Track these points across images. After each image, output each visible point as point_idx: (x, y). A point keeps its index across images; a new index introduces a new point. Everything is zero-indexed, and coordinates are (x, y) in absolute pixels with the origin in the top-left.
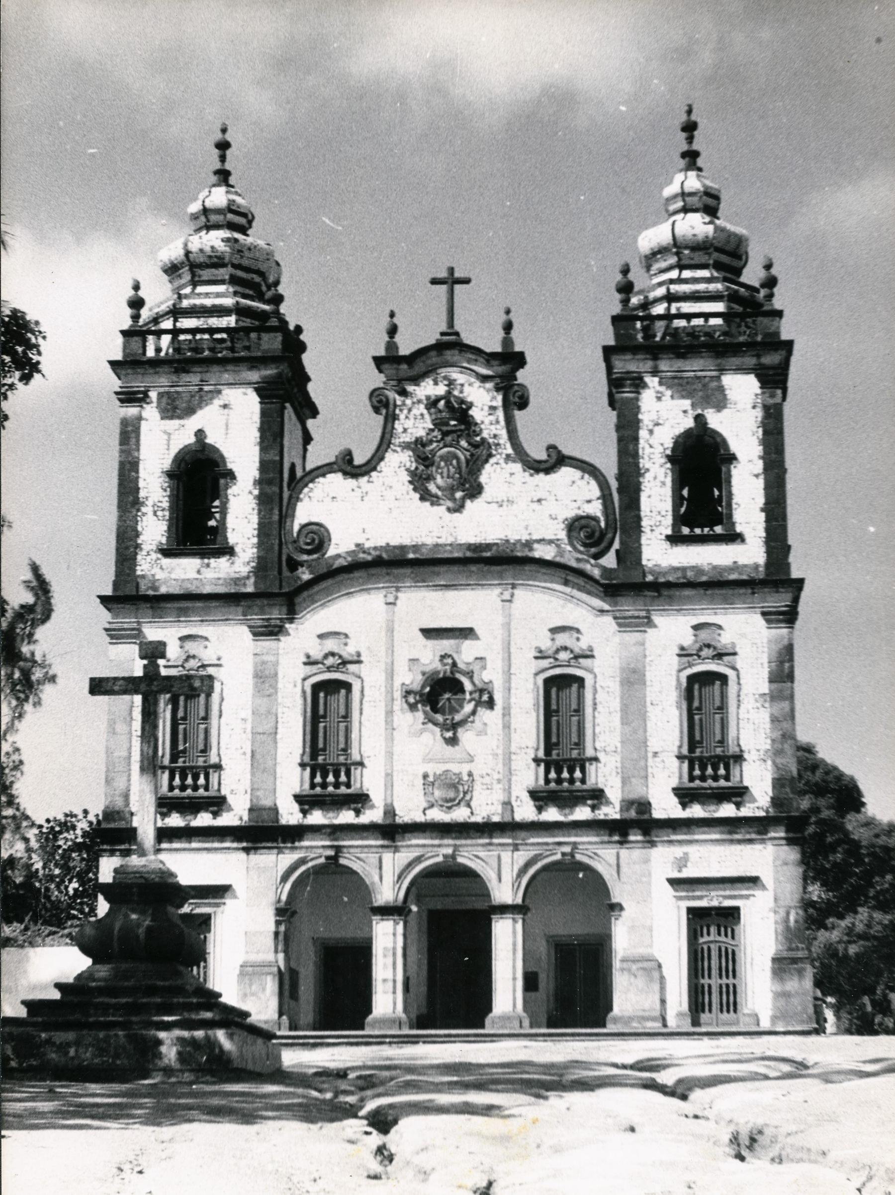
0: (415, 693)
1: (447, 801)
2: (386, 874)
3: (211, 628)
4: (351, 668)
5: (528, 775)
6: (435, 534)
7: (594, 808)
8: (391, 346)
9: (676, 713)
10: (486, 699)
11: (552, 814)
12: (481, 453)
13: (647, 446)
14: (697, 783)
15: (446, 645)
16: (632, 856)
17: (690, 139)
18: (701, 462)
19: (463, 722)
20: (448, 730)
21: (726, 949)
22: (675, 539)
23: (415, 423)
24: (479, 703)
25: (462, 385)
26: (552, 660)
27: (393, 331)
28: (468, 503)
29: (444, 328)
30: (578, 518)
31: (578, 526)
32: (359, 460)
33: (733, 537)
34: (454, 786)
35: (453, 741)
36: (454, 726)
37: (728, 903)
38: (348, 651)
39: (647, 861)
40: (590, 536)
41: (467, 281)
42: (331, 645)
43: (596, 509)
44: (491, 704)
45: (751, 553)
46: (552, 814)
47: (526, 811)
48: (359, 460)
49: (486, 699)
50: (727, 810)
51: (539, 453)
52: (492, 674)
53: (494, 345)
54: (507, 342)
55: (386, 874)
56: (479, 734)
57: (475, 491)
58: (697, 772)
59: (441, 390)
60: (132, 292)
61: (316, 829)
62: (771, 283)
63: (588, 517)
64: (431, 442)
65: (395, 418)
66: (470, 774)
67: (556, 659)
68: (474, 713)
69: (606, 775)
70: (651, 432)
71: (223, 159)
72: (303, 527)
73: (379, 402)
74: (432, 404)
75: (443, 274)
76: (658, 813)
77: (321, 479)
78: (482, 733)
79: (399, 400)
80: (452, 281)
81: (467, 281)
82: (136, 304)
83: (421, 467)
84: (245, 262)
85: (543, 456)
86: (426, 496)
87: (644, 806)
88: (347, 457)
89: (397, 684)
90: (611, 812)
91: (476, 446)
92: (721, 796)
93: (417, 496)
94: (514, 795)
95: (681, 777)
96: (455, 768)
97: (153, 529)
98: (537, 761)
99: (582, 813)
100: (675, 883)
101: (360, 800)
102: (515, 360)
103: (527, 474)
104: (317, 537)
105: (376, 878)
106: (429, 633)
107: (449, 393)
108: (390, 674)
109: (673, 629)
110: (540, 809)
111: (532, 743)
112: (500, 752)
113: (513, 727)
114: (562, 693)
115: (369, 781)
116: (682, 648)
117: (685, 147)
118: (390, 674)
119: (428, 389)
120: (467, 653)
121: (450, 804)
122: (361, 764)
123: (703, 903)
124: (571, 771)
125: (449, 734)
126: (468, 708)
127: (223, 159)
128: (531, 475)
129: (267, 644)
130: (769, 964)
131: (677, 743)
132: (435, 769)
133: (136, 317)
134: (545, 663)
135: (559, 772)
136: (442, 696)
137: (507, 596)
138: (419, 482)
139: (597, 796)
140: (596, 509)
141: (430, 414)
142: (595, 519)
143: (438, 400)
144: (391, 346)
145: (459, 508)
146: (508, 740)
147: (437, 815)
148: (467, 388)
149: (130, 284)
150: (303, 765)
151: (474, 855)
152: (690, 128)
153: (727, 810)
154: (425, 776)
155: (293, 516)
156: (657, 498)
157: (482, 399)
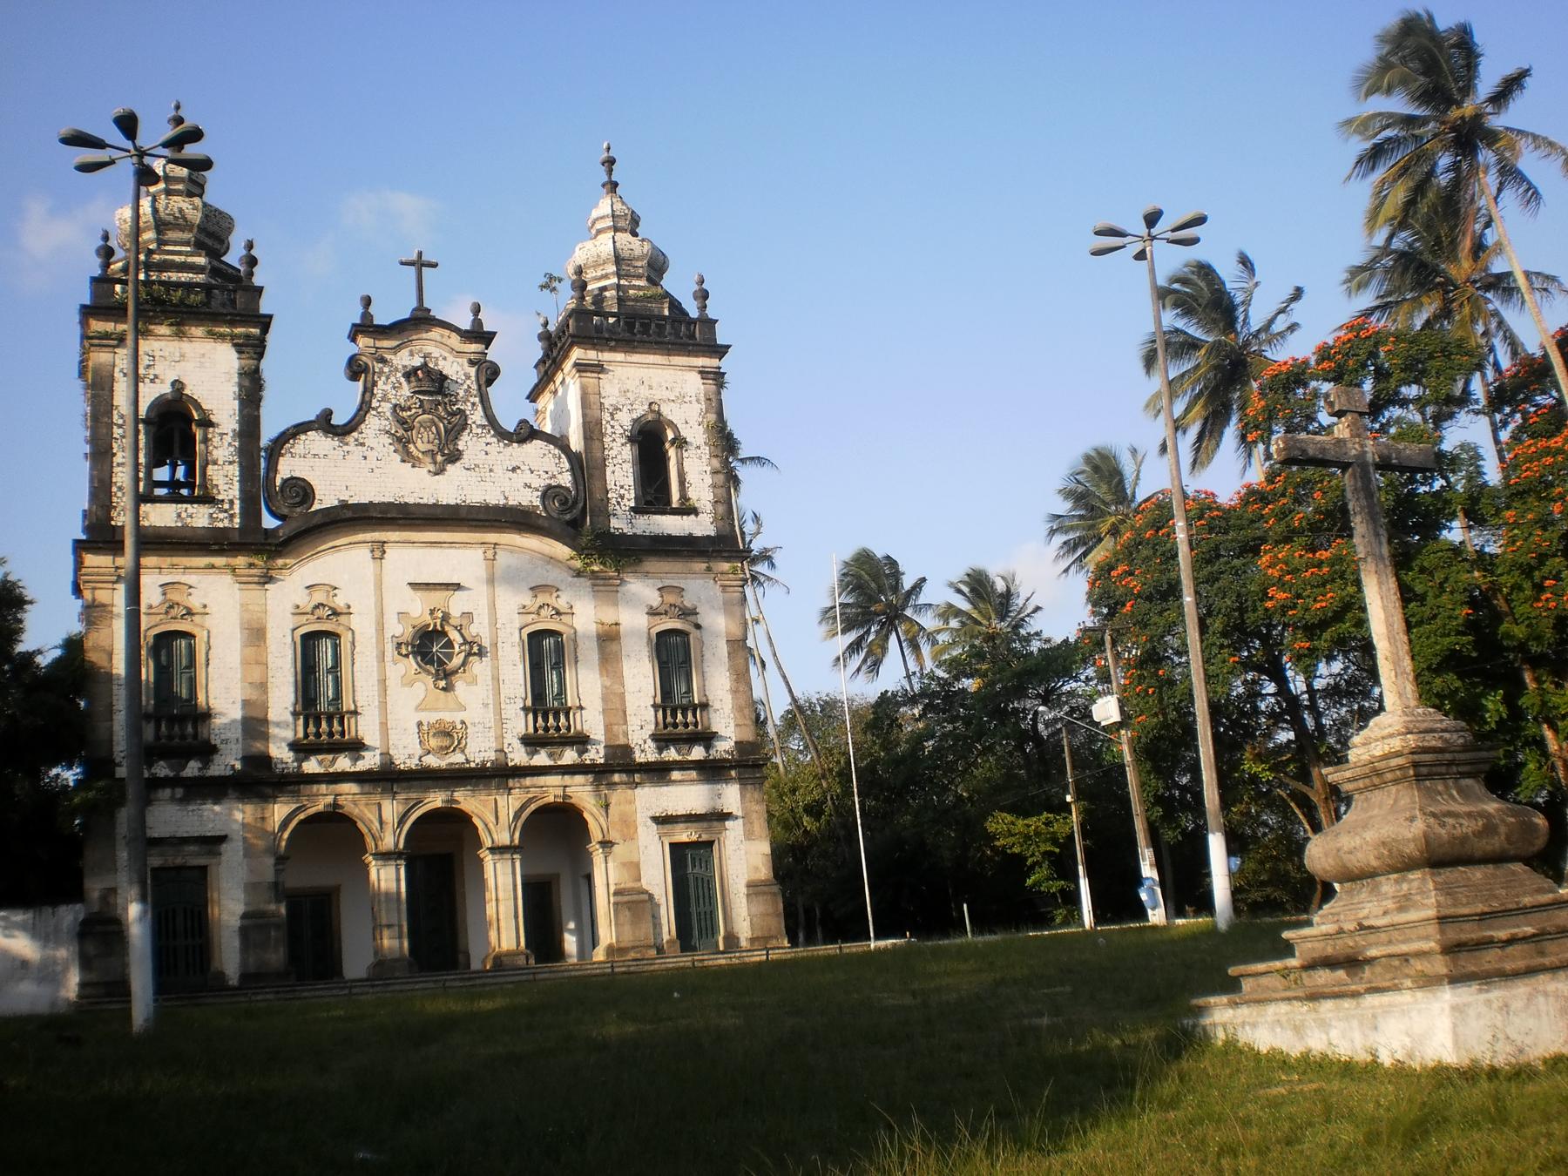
0: (407, 644)
1: (442, 748)
2: (385, 820)
4: (342, 619)
5: (519, 724)
7: (581, 753)
8: (366, 316)
10: (476, 650)
11: (542, 759)
12: (457, 426)
15: (437, 598)
16: (617, 797)
17: (610, 172)
18: (651, 441)
19: (456, 672)
23: (393, 390)
24: (470, 654)
27: (367, 301)
28: (449, 467)
29: (414, 304)
30: (549, 487)
31: (549, 493)
32: (338, 420)
33: (688, 510)
34: (449, 734)
36: (448, 675)
38: (339, 602)
39: (631, 802)
40: (564, 503)
41: (435, 265)
42: (319, 597)
44: (481, 653)
46: (542, 759)
47: (518, 756)
48: (338, 420)
49: (476, 650)
50: (698, 753)
51: (510, 427)
52: (479, 629)
53: (465, 323)
54: (477, 323)
55: (385, 820)
56: (469, 684)
57: (454, 457)
58: (669, 719)
59: (417, 361)
60: (101, 243)
61: (315, 779)
62: (703, 296)
63: (559, 486)
64: (410, 409)
65: (375, 384)
66: (463, 722)
68: (464, 664)
69: (591, 722)
72: (285, 481)
73: (356, 369)
74: (410, 374)
75: (414, 257)
76: (640, 758)
77: (303, 437)
78: (474, 681)
79: (378, 366)
80: (420, 264)
81: (435, 265)
82: (107, 253)
83: (401, 432)
84: (211, 228)
85: (510, 427)
86: (407, 457)
87: (627, 750)
88: (327, 414)
89: (388, 635)
90: (596, 755)
91: (453, 414)
93: (398, 458)
94: (506, 742)
95: (657, 724)
96: (447, 717)
98: (525, 709)
99: (569, 756)
100: (656, 820)
101: (356, 747)
102: (486, 338)
104: (302, 490)
106: (415, 586)
107: (425, 364)
108: (381, 627)
110: (532, 754)
111: (521, 692)
115: (366, 728)
117: (606, 179)
118: (381, 627)
119: (406, 359)
120: (457, 605)
121: (444, 750)
122: (355, 713)
124: (557, 719)
125: (442, 684)
126: (457, 661)
129: (254, 593)
130: (744, 890)
132: (430, 717)
133: (106, 265)
135: (546, 720)
136: (430, 647)
137: (490, 554)
138: (403, 444)
139: (581, 741)
140: (566, 480)
141: (409, 382)
142: (567, 489)
143: (416, 369)
144: (366, 316)
145: (440, 471)
146: (497, 692)
147: (433, 761)
148: (441, 363)
151: (469, 801)
152: (610, 163)
154: (420, 724)
155: (276, 471)
156: (621, 475)
157: (456, 368)
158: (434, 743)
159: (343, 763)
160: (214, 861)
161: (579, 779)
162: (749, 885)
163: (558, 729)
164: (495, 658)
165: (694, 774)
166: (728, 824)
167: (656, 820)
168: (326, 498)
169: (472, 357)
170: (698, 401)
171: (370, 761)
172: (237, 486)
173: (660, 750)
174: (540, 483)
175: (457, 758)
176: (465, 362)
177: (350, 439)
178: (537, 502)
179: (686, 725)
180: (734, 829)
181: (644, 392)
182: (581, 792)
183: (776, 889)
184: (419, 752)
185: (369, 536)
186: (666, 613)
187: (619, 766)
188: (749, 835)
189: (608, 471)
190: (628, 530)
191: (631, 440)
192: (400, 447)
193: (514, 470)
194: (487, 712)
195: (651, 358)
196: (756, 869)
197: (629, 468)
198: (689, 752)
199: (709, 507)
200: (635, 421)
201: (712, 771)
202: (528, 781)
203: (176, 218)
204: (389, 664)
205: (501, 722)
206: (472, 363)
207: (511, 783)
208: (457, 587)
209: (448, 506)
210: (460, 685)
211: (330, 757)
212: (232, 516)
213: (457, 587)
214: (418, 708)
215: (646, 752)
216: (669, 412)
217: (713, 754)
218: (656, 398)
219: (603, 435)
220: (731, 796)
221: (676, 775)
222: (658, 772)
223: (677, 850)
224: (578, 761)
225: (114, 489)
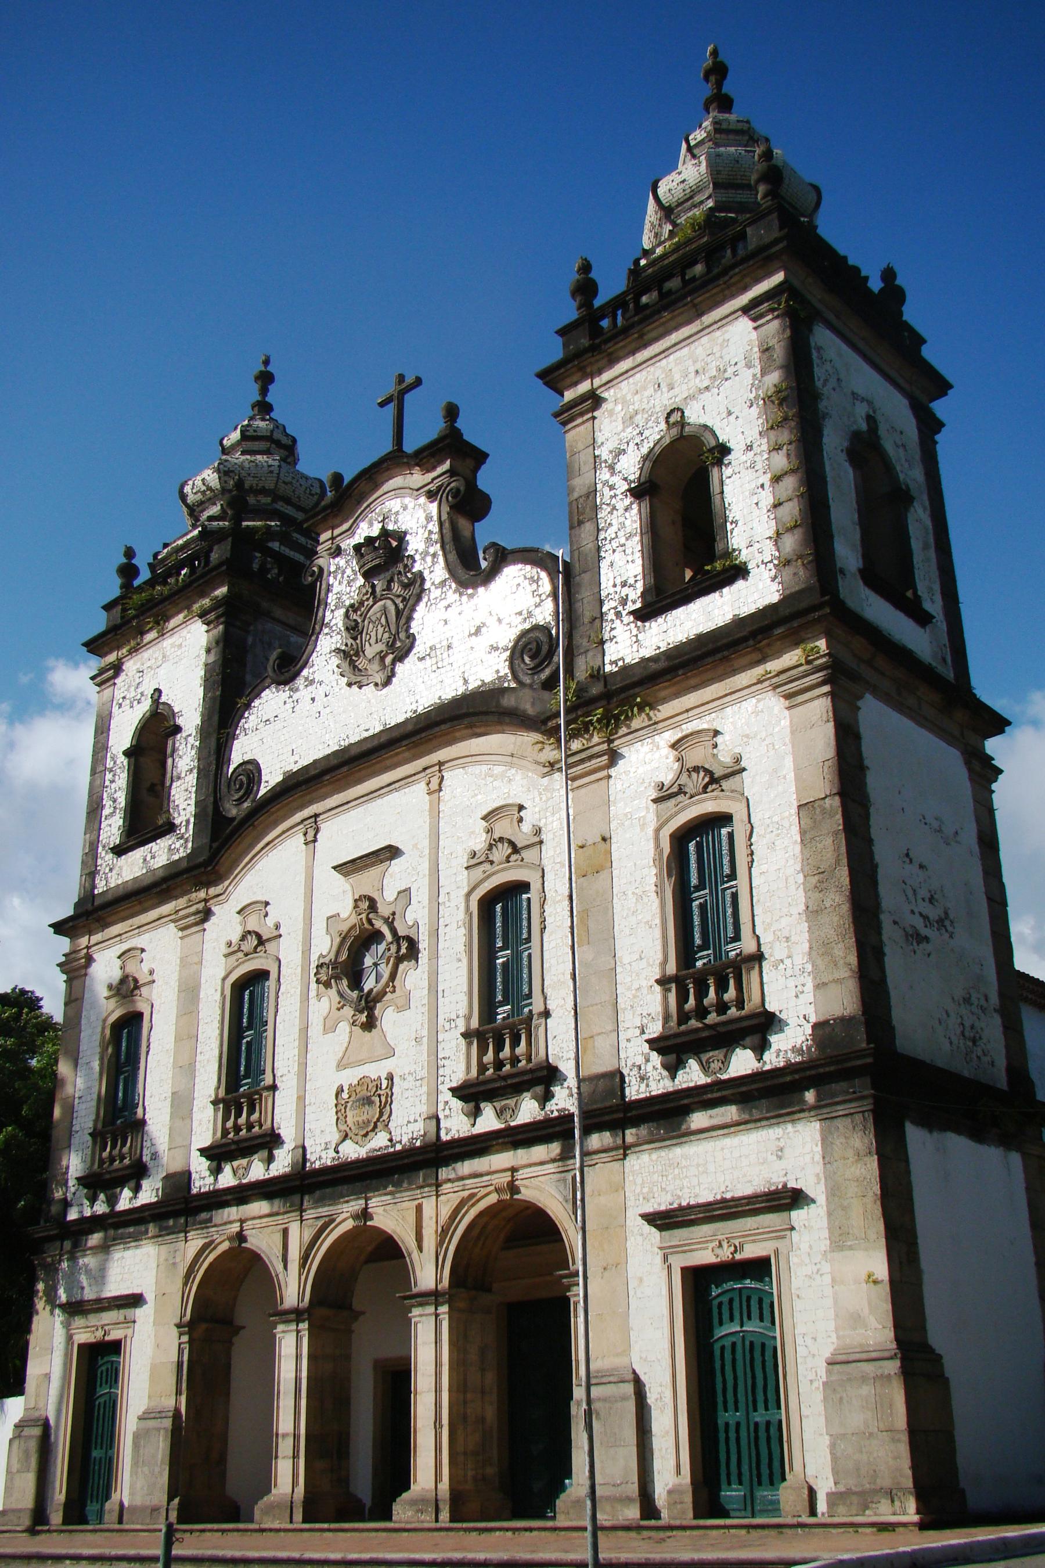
3: (147, 936)
6: (362, 728)
9: (655, 903)
13: (606, 490)
14: (694, 1023)
20: (361, 1012)
21: (763, 1345)
22: (645, 614)
24: (399, 960)
25: (397, 513)
26: (487, 866)
35: (370, 1025)
37: (751, 1251)
43: (545, 614)
45: (757, 592)
47: (457, 1124)
50: (742, 1062)
56: (400, 1009)
59: (375, 532)
60: (124, 560)
63: (536, 628)
67: (492, 862)
68: (393, 976)
70: (612, 468)
71: (264, 391)
76: (634, 1091)
90: (565, 1099)
92: (726, 1039)
95: (667, 1018)
97: (112, 829)
98: (466, 1035)
103: (465, 598)
105: (280, 1267)
109: (647, 759)
112: (425, 1033)
113: (440, 989)
114: (502, 913)
116: (661, 786)
122: (274, 1088)
123: (706, 1257)
127: (264, 391)
128: (471, 596)
131: (659, 956)
132: (349, 1077)
134: (478, 873)
147: (352, 1151)
149: (123, 550)
150: (215, 1103)
151: (391, 1213)
153: (742, 1062)
154: (340, 1091)
158: (353, 1116)
159: (257, 1171)
160: (129, 1332)
161: (540, 1152)
162: (830, 1363)
163: (515, 1060)
164: (435, 956)
165: (730, 1112)
166: (797, 1216)
167: (664, 1220)
168: (271, 778)
169: (432, 487)
170: (749, 366)
171: (282, 1163)
172: (193, 796)
173: (673, 1069)
174: (507, 635)
175: (379, 1141)
176: (423, 500)
177: (300, 682)
178: (505, 670)
179: (722, 1007)
180: (810, 1223)
181: (664, 401)
182: (539, 1178)
183: (893, 1367)
184: (336, 1137)
185: (298, 817)
186: (681, 791)
187: (616, 1114)
188: (840, 1240)
189: (604, 565)
190: (632, 657)
191: (637, 492)
192: (345, 665)
193: (478, 632)
194: (420, 1053)
195: (674, 337)
196: (856, 1320)
197: (635, 545)
198: (726, 1062)
199: (769, 550)
200: (645, 458)
201: (770, 1096)
202: (467, 1167)
203: (203, 493)
204: (313, 1001)
205: (435, 1063)
206: (431, 495)
207: (444, 1173)
208: (392, 852)
209: (397, 725)
210: (388, 1017)
211: (244, 1162)
212: (187, 841)
213: (392, 852)
214: (341, 1066)
215: (648, 1079)
216: (695, 415)
217: (772, 1060)
218: (678, 402)
219: (596, 508)
220: (795, 1150)
221: (698, 1120)
222: (667, 1116)
223: (699, 1283)
224: (540, 1116)
225: (100, 849)
